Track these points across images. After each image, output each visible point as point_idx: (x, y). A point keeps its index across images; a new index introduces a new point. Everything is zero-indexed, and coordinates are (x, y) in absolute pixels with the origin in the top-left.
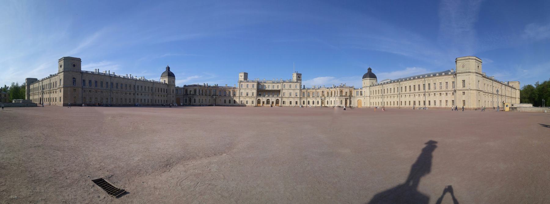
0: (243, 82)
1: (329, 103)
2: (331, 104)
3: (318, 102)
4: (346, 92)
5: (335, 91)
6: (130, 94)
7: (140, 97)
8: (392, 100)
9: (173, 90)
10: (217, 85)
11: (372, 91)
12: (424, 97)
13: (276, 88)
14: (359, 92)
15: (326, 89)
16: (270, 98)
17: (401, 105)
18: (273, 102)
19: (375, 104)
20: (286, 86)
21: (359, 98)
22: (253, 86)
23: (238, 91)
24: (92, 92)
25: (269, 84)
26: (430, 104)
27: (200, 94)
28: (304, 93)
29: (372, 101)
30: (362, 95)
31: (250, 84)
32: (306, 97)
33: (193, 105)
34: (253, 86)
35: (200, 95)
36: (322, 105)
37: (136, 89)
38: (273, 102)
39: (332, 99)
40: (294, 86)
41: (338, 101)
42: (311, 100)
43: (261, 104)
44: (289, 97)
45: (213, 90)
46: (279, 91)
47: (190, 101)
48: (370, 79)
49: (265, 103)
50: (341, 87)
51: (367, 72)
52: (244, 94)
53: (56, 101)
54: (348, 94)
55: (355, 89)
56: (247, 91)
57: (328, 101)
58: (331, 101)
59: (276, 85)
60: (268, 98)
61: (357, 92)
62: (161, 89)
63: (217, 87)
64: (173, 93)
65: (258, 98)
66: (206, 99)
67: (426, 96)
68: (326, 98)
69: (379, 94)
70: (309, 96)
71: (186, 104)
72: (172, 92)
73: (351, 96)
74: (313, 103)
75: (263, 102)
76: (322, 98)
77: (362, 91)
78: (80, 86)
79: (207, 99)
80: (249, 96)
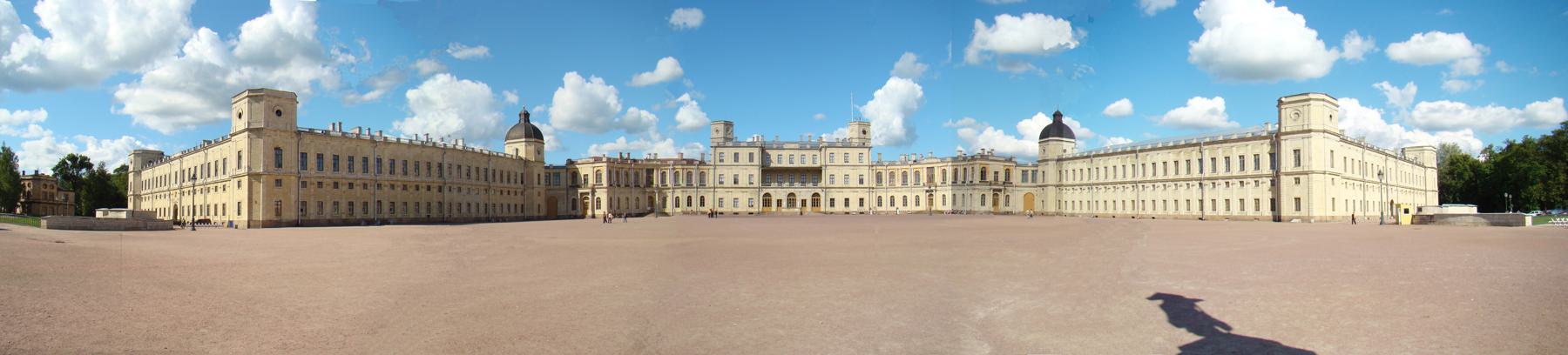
4: (996, 173)
5: (965, 169)
6: (429, 188)
7: (455, 197)
9: (539, 175)
10: (656, 154)
13: (809, 164)
15: (938, 163)
18: (804, 202)
23: (712, 171)
24: (324, 186)
25: (792, 152)
31: (744, 153)
34: (751, 159)
37: (446, 174)
38: (804, 202)
42: (899, 193)
43: (774, 207)
49: (784, 203)
52: (729, 182)
53: (224, 214)
54: (1002, 178)
55: (1017, 165)
56: (735, 171)
59: (809, 154)
60: (792, 191)
62: (509, 173)
64: (539, 183)
65: (765, 191)
71: (573, 213)
72: (536, 181)
75: (779, 202)
77: (1037, 171)
78: (293, 170)
79: (630, 197)
80: (740, 185)
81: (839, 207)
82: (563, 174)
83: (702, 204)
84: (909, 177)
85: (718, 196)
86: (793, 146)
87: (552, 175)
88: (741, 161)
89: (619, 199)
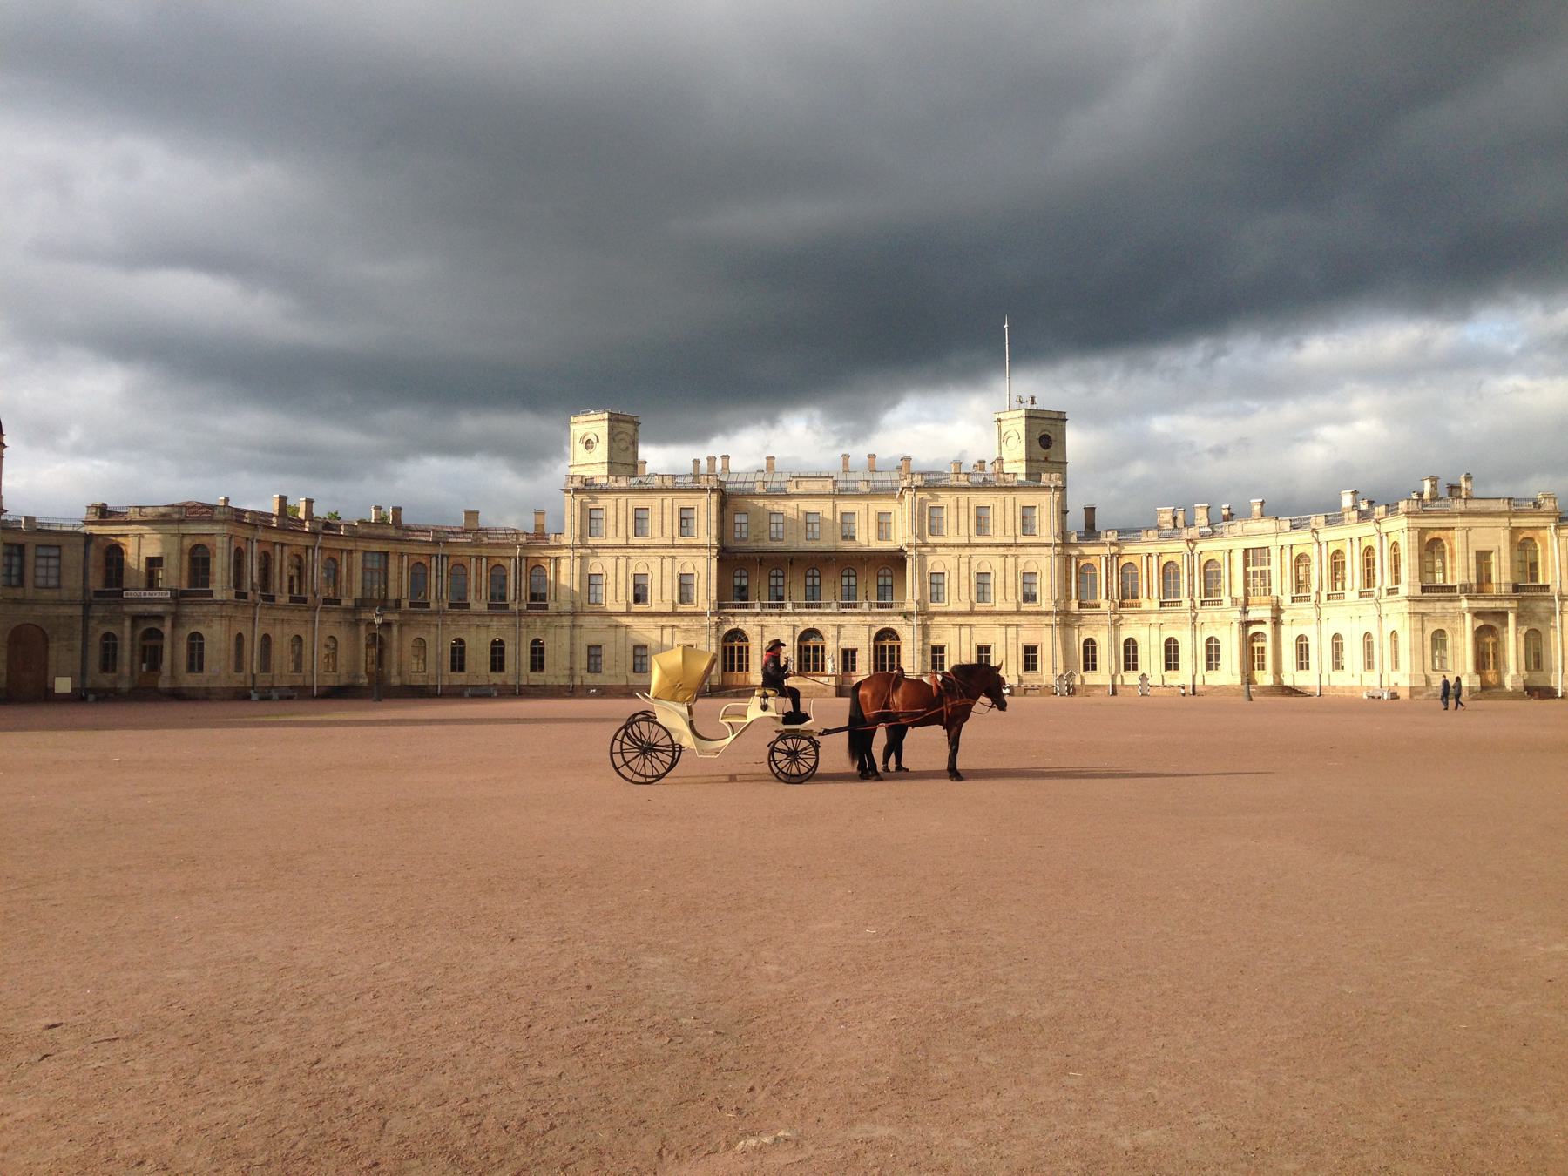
1: (1320, 653)
2: (1338, 665)
4: (1483, 557)
10: (397, 511)
13: (866, 539)
16: (824, 624)
20: (953, 520)
27: (247, 588)
28: (1086, 573)
31: (662, 509)
32: (1105, 605)
33: (178, 695)
34: (685, 520)
35: (241, 595)
36: (1249, 679)
38: (849, 657)
40: (1009, 518)
44: (971, 613)
47: (151, 653)
54: (1502, 572)
58: (1337, 637)
63: (392, 532)
66: (298, 637)
71: (105, 680)
74: (1171, 661)
76: (1252, 615)
80: (654, 604)
82: (73, 556)
83: (537, 663)
84: (1184, 578)
86: (815, 486)
87: (30, 553)
89: (266, 639)
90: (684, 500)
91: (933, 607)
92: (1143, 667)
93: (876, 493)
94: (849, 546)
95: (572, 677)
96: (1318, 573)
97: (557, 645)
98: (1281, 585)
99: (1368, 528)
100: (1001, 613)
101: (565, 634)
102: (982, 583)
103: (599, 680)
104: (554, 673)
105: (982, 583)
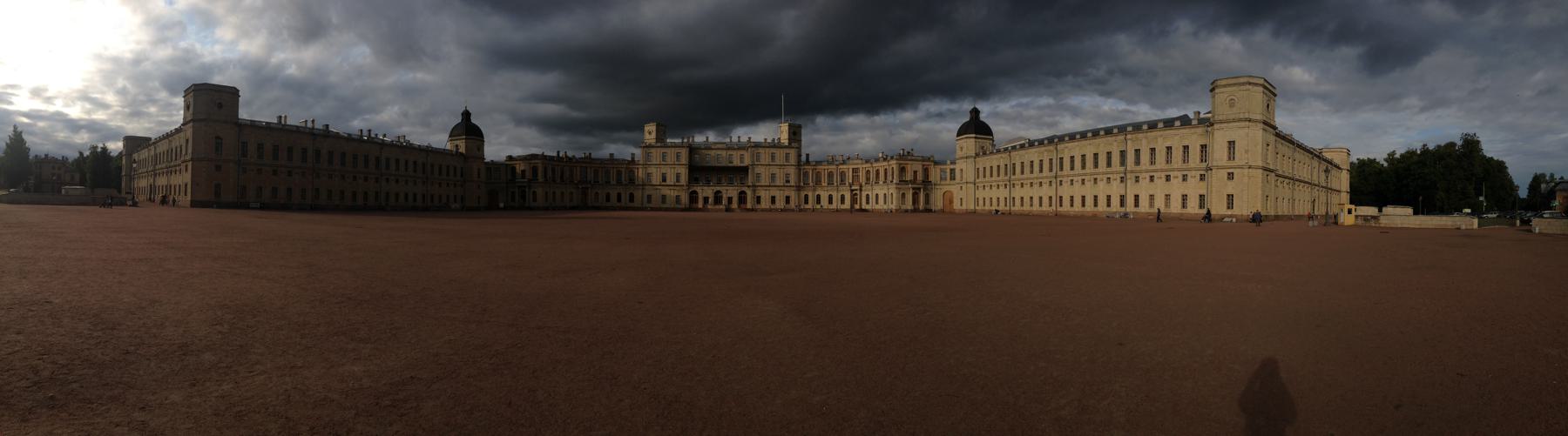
0: (653, 147)
2: (877, 203)
3: (843, 198)
4: (915, 172)
8: (1036, 192)
11: (981, 170)
12: (1123, 185)
13: (736, 163)
14: (948, 171)
15: (862, 164)
17: (1061, 206)
18: (730, 200)
19: (988, 202)
21: (946, 188)
22: (678, 156)
26: (1137, 204)
28: (806, 174)
29: (981, 194)
30: (954, 179)
31: (671, 153)
32: (811, 184)
34: (678, 156)
36: (852, 206)
38: (730, 200)
39: (880, 190)
41: (894, 195)
43: (700, 205)
44: (770, 186)
45: (578, 168)
46: (743, 171)
48: (975, 138)
50: (901, 157)
51: (967, 119)
54: (920, 177)
55: (936, 163)
57: (868, 195)
58: (877, 195)
60: (718, 188)
61: (943, 171)
67: (1129, 181)
68: (863, 188)
69: (999, 175)
70: (818, 182)
73: (926, 182)
74: (830, 201)
76: (853, 188)
80: (668, 182)
81: (765, 204)
84: (835, 176)
85: (647, 193)
88: (669, 161)
90: (678, 150)
91: (757, 184)
92: (822, 203)
93: (739, 149)
94: (731, 165)
95: (642, 204)
96: (872, 176)
97: (638, 194)
98: (862, 179)
99: (885, 163)
100: (779, 186)
101: (640, 192)
102: (773, 176)
103: (651, 205)
104: (637, 203)
105: (773, 176)
